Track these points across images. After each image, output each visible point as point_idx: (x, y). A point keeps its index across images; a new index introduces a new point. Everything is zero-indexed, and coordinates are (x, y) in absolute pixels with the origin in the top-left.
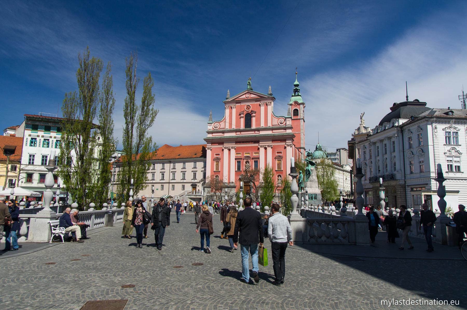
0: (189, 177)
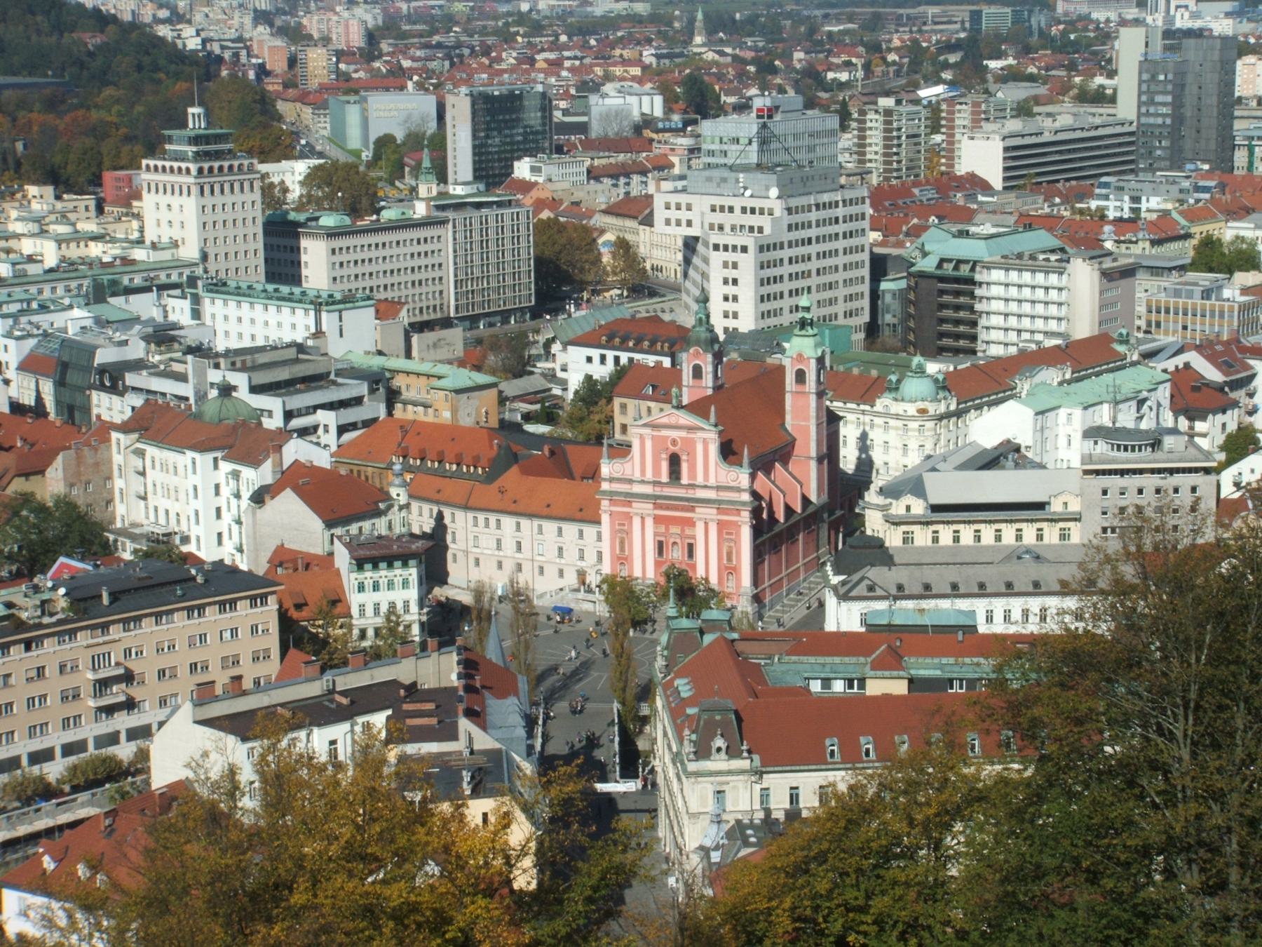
0: (571, 555)
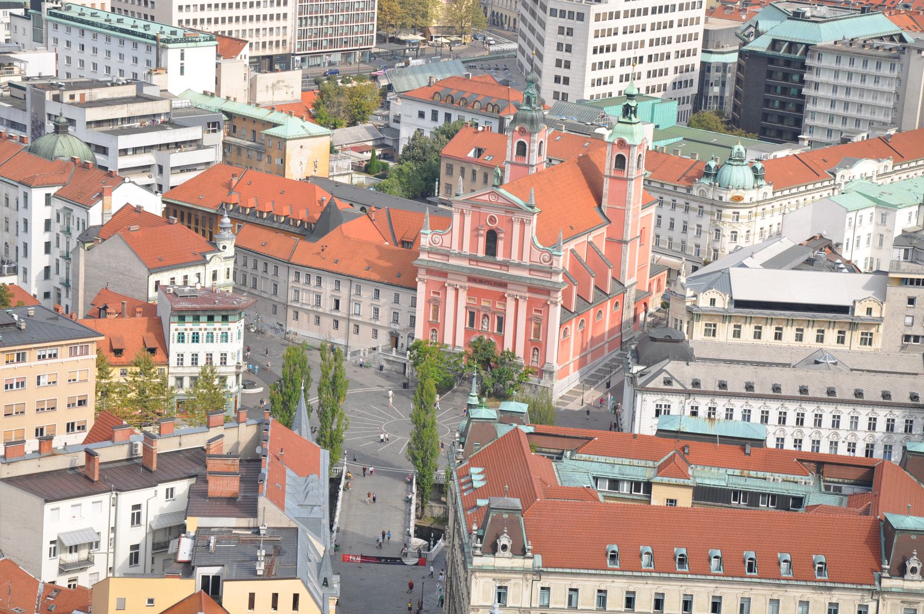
0: (385, 318)
